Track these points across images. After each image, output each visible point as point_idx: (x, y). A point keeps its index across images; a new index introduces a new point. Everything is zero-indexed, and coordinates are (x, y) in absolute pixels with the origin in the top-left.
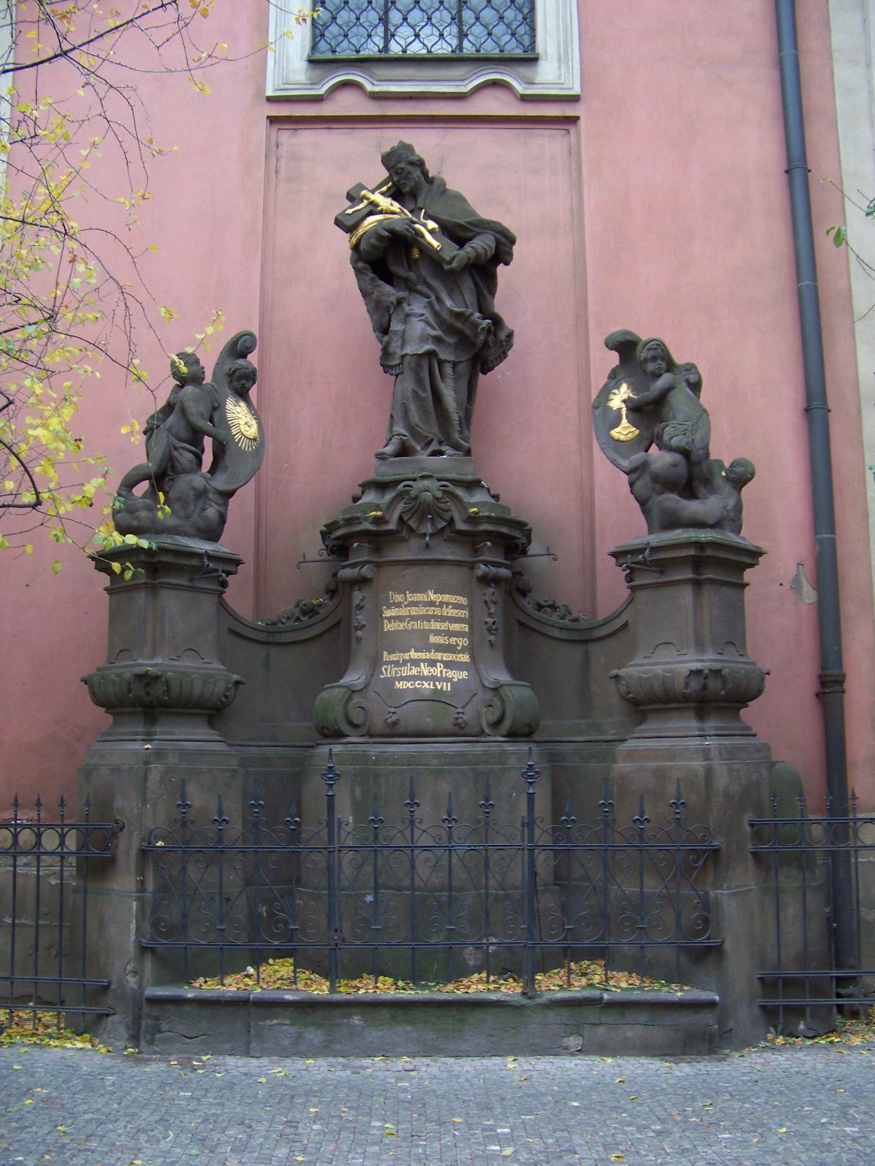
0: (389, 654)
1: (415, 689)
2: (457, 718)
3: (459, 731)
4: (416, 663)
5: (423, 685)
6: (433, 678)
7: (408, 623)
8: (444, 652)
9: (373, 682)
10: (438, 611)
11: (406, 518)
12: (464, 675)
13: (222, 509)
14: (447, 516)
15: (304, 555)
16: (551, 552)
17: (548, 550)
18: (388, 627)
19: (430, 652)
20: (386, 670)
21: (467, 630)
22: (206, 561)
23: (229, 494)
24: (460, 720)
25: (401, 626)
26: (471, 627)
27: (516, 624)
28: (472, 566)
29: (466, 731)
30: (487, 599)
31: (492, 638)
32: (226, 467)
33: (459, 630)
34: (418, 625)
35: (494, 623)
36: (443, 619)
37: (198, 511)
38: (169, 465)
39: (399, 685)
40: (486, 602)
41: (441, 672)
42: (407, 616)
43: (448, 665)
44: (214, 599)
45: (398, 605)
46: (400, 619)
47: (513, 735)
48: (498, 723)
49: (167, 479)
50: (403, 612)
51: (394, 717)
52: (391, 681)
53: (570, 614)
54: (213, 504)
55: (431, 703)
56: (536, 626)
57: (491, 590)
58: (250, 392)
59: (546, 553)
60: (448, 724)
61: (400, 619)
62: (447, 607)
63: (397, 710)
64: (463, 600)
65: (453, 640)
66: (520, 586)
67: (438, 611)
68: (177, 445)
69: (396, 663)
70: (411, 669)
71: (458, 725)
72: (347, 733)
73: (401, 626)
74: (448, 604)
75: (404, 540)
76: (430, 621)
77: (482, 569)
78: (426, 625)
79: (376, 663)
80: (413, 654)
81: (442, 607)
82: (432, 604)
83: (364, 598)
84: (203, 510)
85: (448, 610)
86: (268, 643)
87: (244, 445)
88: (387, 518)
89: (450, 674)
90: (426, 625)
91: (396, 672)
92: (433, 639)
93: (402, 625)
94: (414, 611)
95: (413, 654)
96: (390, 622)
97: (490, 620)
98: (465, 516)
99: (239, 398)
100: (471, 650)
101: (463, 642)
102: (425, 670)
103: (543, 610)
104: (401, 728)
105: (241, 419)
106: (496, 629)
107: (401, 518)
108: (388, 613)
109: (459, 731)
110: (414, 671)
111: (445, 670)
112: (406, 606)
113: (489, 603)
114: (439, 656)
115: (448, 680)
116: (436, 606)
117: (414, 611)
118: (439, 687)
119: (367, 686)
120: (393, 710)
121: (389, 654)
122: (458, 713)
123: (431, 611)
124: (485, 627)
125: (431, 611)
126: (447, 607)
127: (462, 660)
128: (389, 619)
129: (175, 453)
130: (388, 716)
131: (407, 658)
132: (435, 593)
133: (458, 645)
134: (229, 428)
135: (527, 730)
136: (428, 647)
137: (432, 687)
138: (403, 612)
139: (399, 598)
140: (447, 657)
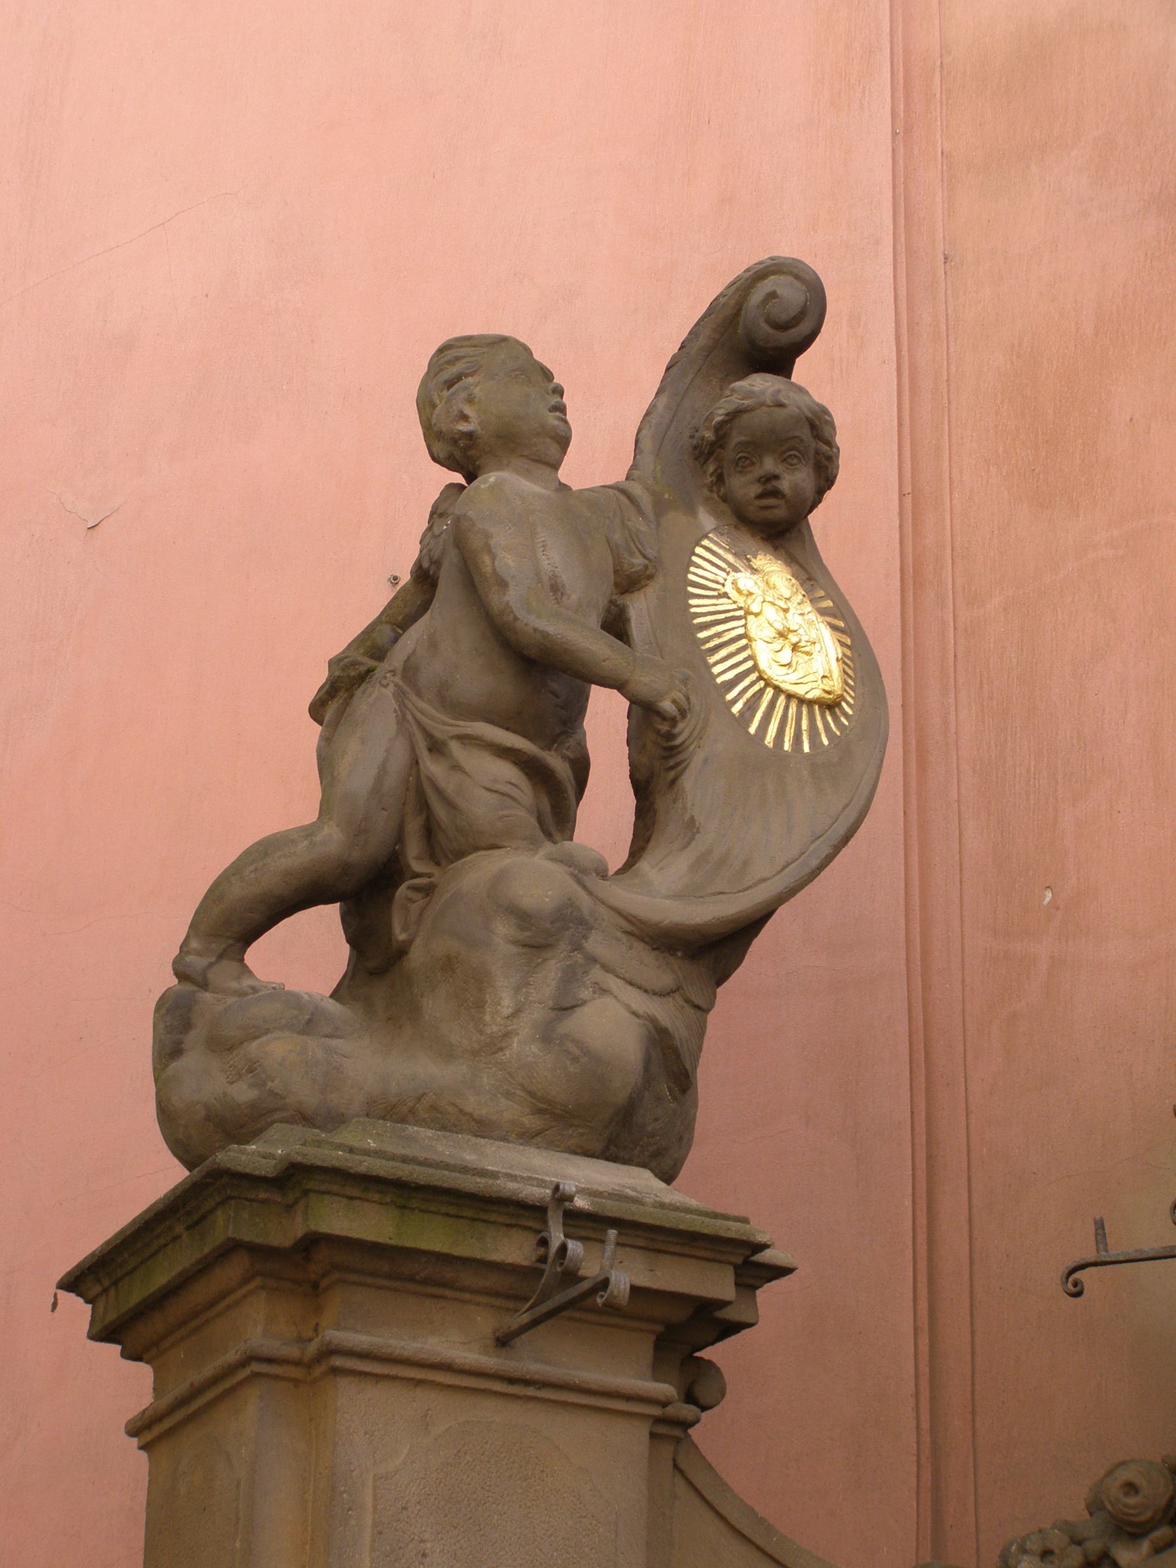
13: (664, 1012)
15: (1100, 1225)
22: (557, 1236)
23: (714, 950)
32: (692, 827)
37: (536, 1013)
38: (414, 827)
44: (632, 1438)
49: (402, 891)
54: (613, 983)
58: (815, 519)
68: (440, 731)
84: (564, 1008)
87: (775, 730)
99: (748, 541)
105: (767, 630)
129: (434, 768)
134: (696, 658)
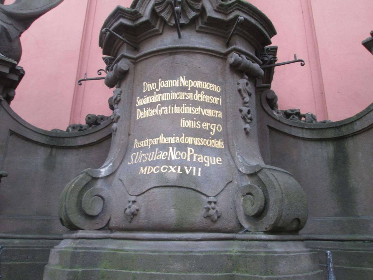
0: (139, 142)
1: (161, 174)
2: (208, 209)
3: (211, 225)
4: (165, 147)
5: (169, 169)
6: (182, 163)
7: (159, 108)
8: (195, 136)
9: (121, 169)
10: (190, 96)
11: (158, 11)
12: (217, 160)
14: (199, 6)
16: (298, 59)
17: (295, 57)
18: (141, 115)
19: (180, 137)
20: (134, 157)
21: (220, 116)
24: (212, 212)
25: (151, 113)
26: (225, 115)
27: (267, 129)
28: (224, 56)
29: (218, 225)
30: (240, 87)
31: (247, 126)
33: (212, 115)
34: (167, 110)
35: (249, 112)
36: (195, 104)
39: (143, 171)
40: (240, 91)
41: (192, 156)
42: (158, 103)
43: (200, 149)
45: (151, 93)
46: (152, 106)
47: (277, 230)
48: (259, 215)
50: (155, 98)
51: (134, 207)
52: (137, 167)
53: (316, 120)
55: (177, 189)
56: (286, 130)
57: (245, 81)
59: (293, 59)
60: (198, 216)
61: (152, 106)
62: (199, 93)
63: (139, 199)
64: (216, 88)
65: (206, 125)
66: (269, 97)
67: (190, 96)
69: (144, 150)
70: (158, 154)
71: (208, 217)
72: (79, 225)
73: (151, 113)
74: (200, 90)
75: (158, 34)
76: (181, 106)
77: (234, 57)
78: (177, 110)
79: (127, 149)
80: (163, 139)
81: (194, 93)
82: (184, 89)
83: (121, 92)
85: (201, 96)
86: (52, 147)
88: (141, 12)
89: (201, 159)
90: (177, 110)
91: (143, 158)
92: (185, 123)
93: (153, 112)
94: (165, 97)
95: (163, 139)
96: (142, 110)
97: (245, 110)
98: (216, 5)
100: (223, 136)
101: (216, 128)
102: (173, 155)
103: (291, 117)
104: (141, 220)
106: (251, 119)
107: (153, 11)
108: (141, 102)
109: (211, 225)
110: (162, 156)
111: (195, 155)
112: (157, 93)
113: (243, 93)
114: (190, 140)
115: (198, 164)
116: (188, 92)
117: (165, 97)
118: (188, 172)
119: (112, 175)
120: (133, 198)
121: (139, 142)
122: (210, 202)
123: (182, 96)
124: (240, 115)
125: (182, 96)
126: (199, 93)
127: (215, 146)
128: (141, 108)
130: (127, 206)
131: (156, 143)
132: (187, 79)
133: (211, 130)
135: (294, 226)
136: (179, 131)
137: (179, 171)
138: (155, 98)
139: (151, 86)
140: (197, 141)
